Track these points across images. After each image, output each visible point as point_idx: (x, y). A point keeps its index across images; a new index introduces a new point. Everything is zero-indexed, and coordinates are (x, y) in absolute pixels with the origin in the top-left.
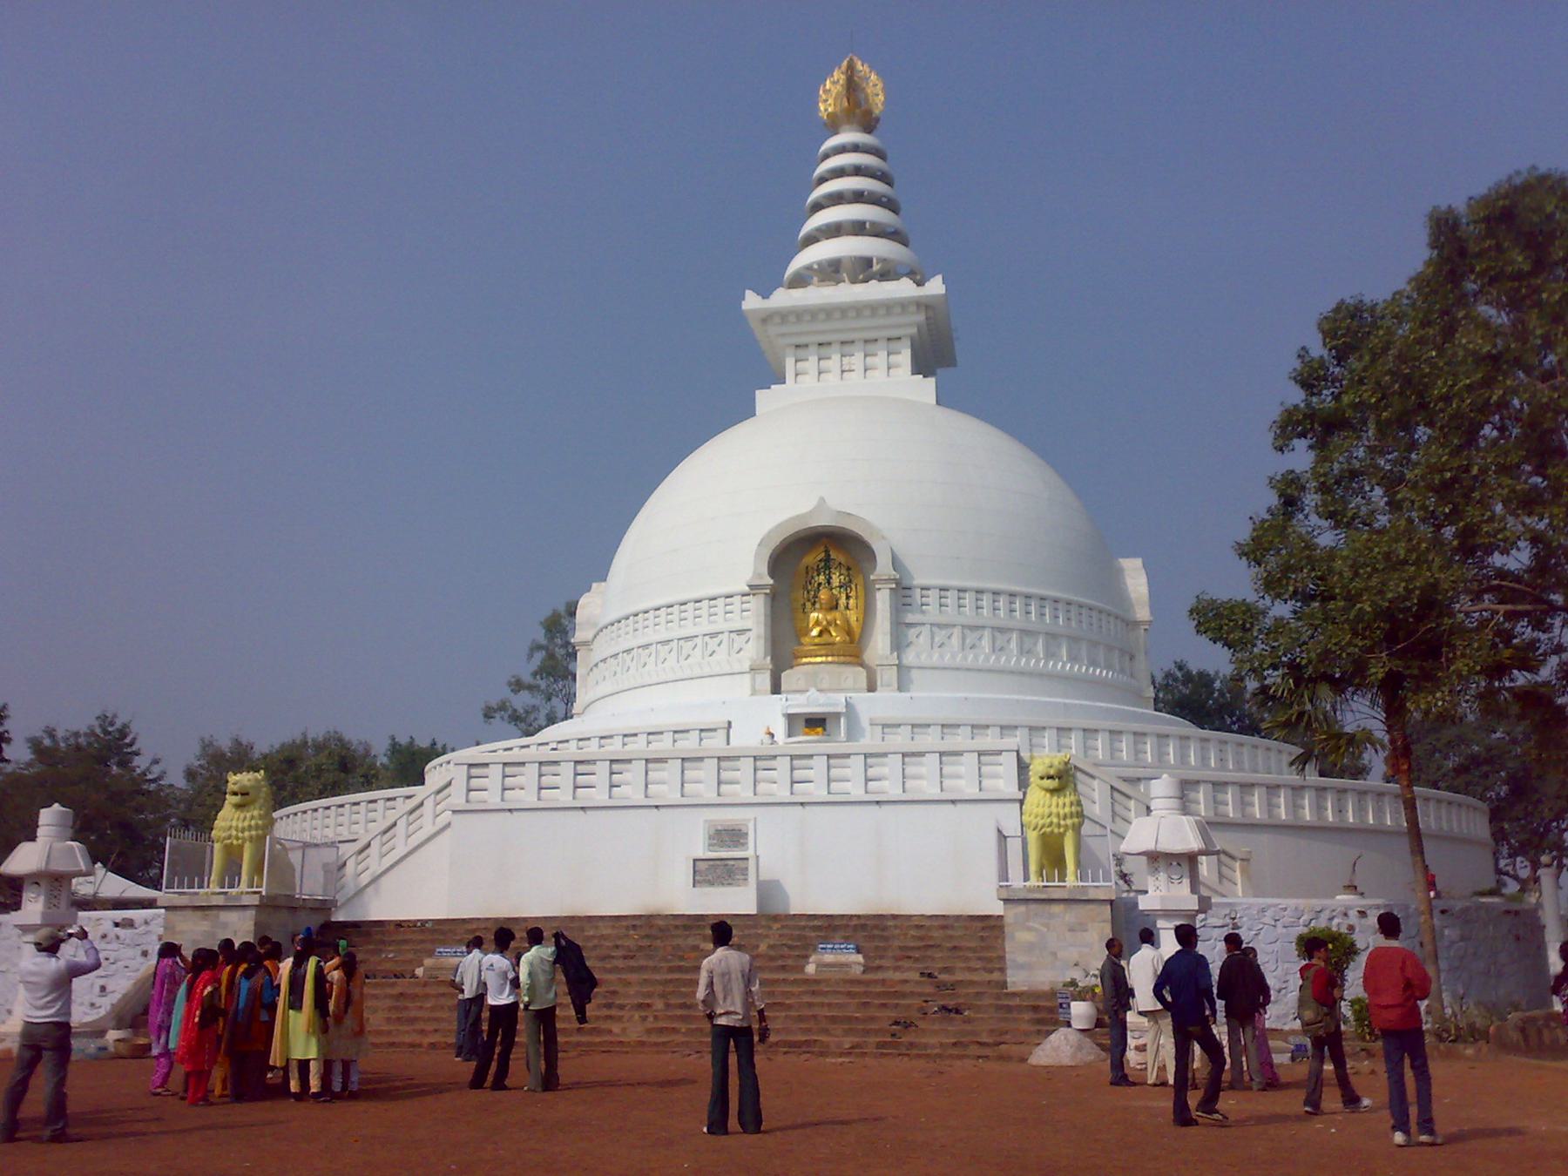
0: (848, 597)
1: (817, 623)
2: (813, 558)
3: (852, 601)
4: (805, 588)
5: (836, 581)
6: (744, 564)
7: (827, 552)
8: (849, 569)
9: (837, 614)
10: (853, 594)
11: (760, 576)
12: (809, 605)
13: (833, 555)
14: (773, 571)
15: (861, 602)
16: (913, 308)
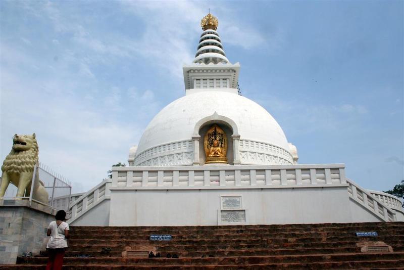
0: (222, 144)
1: (213, 151)
2: (211, 131)
3: (223, 145)
4: (208, 140)
5: (218, 139)
6: (192, 130)
7: (215, 129)
8: (222, 135)
9: (219, 148)
10: (223, 143)
11: (196, 135)
12: (209, 146)
13: (217, 130)
14: (200, 133)
15: (226, 146)
16: (231, 71)
